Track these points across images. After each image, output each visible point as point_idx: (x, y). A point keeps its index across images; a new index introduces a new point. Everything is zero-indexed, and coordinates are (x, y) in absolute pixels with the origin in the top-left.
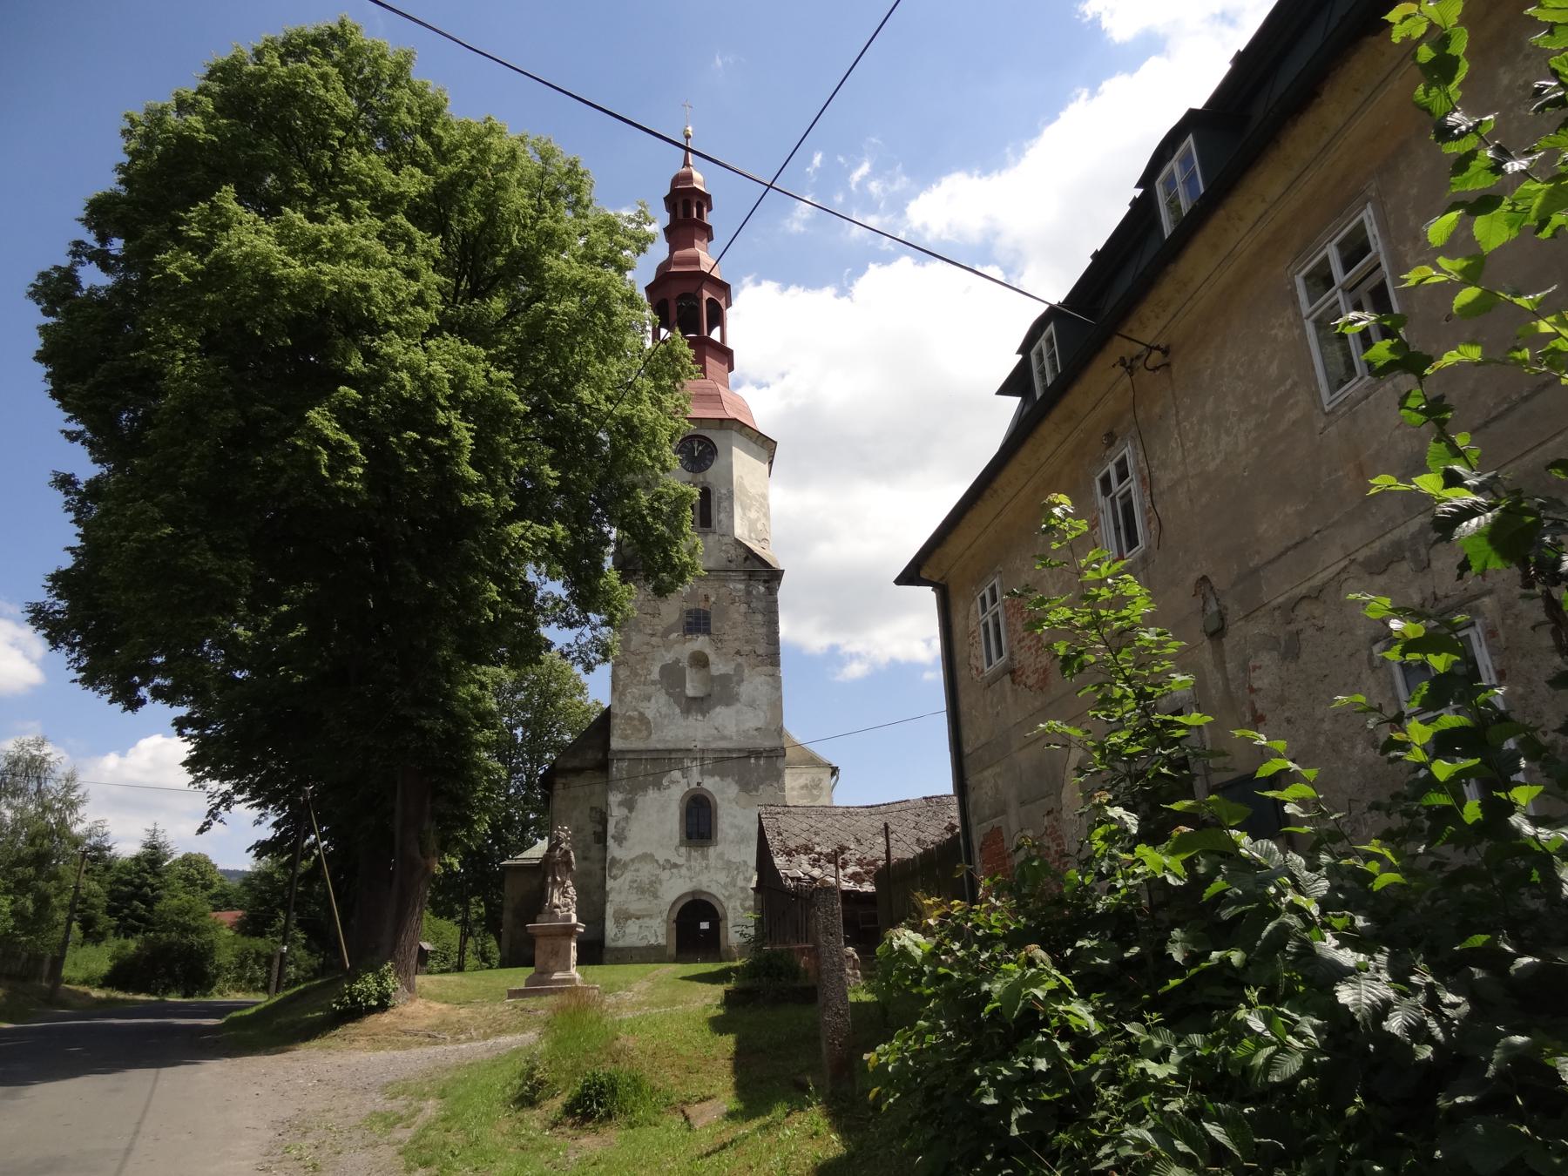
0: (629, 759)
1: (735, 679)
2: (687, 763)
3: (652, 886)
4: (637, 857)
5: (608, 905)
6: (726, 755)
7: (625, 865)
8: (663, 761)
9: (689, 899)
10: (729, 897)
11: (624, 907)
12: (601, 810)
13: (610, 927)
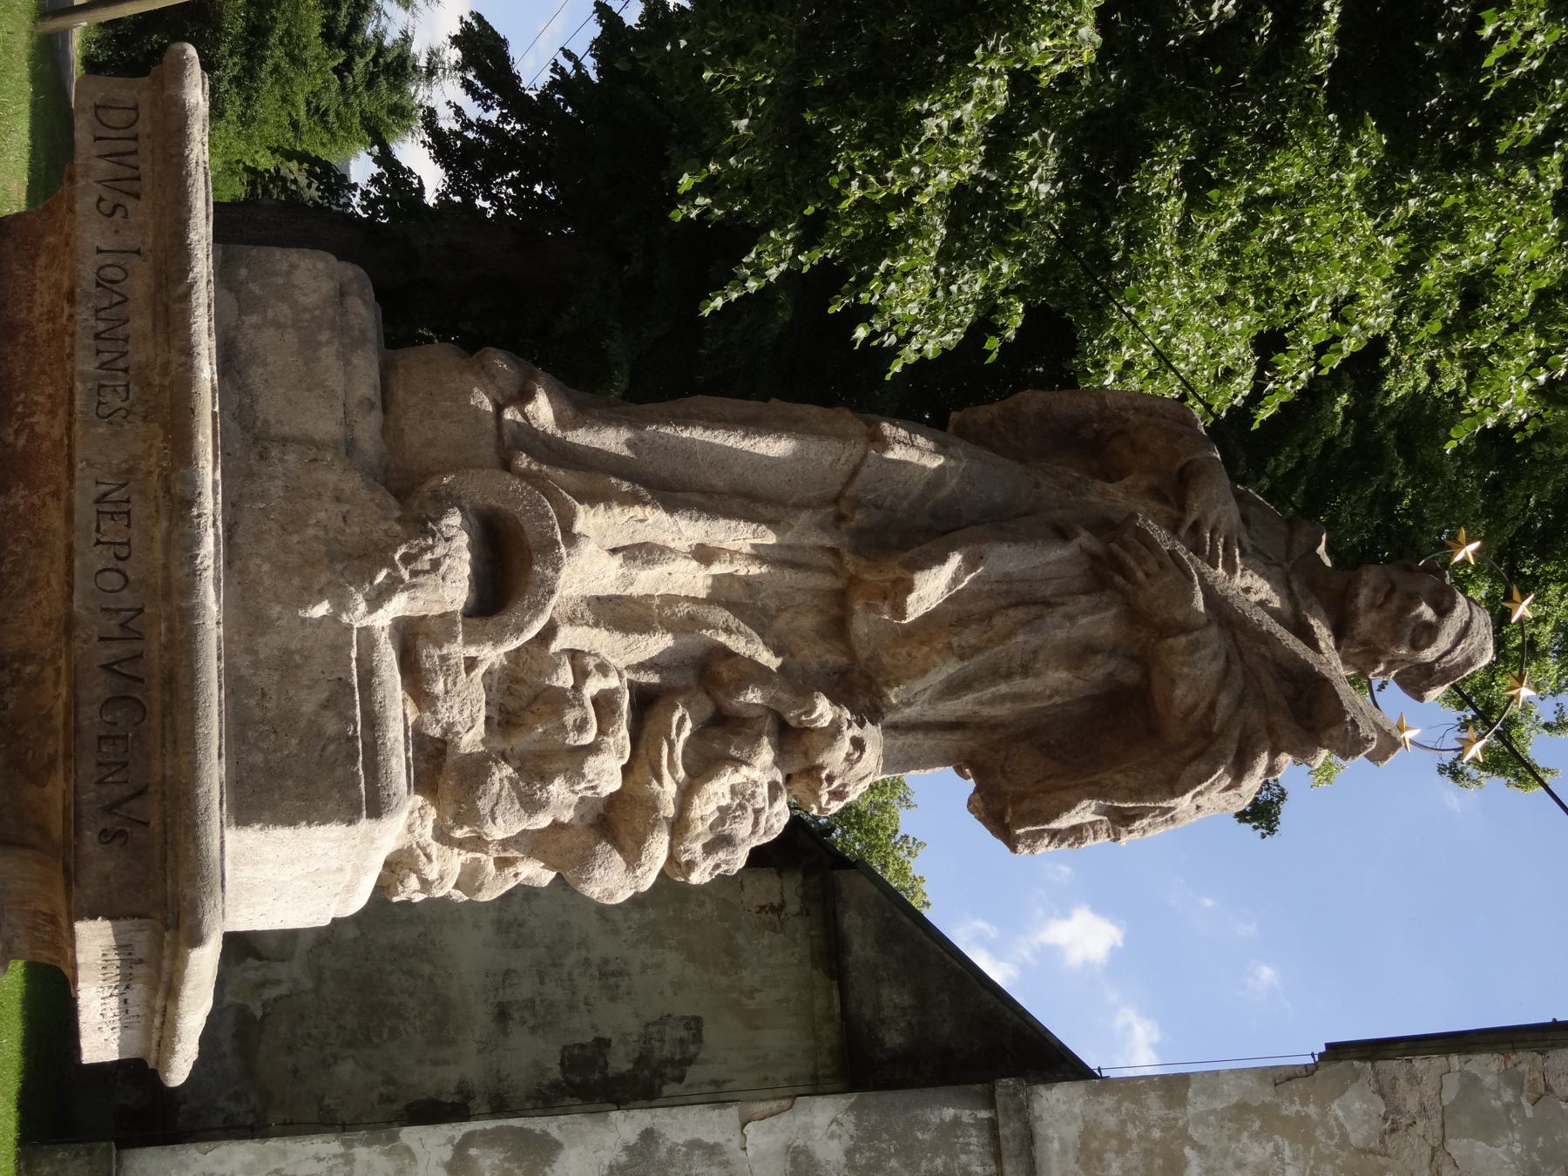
12: (690, 1061)
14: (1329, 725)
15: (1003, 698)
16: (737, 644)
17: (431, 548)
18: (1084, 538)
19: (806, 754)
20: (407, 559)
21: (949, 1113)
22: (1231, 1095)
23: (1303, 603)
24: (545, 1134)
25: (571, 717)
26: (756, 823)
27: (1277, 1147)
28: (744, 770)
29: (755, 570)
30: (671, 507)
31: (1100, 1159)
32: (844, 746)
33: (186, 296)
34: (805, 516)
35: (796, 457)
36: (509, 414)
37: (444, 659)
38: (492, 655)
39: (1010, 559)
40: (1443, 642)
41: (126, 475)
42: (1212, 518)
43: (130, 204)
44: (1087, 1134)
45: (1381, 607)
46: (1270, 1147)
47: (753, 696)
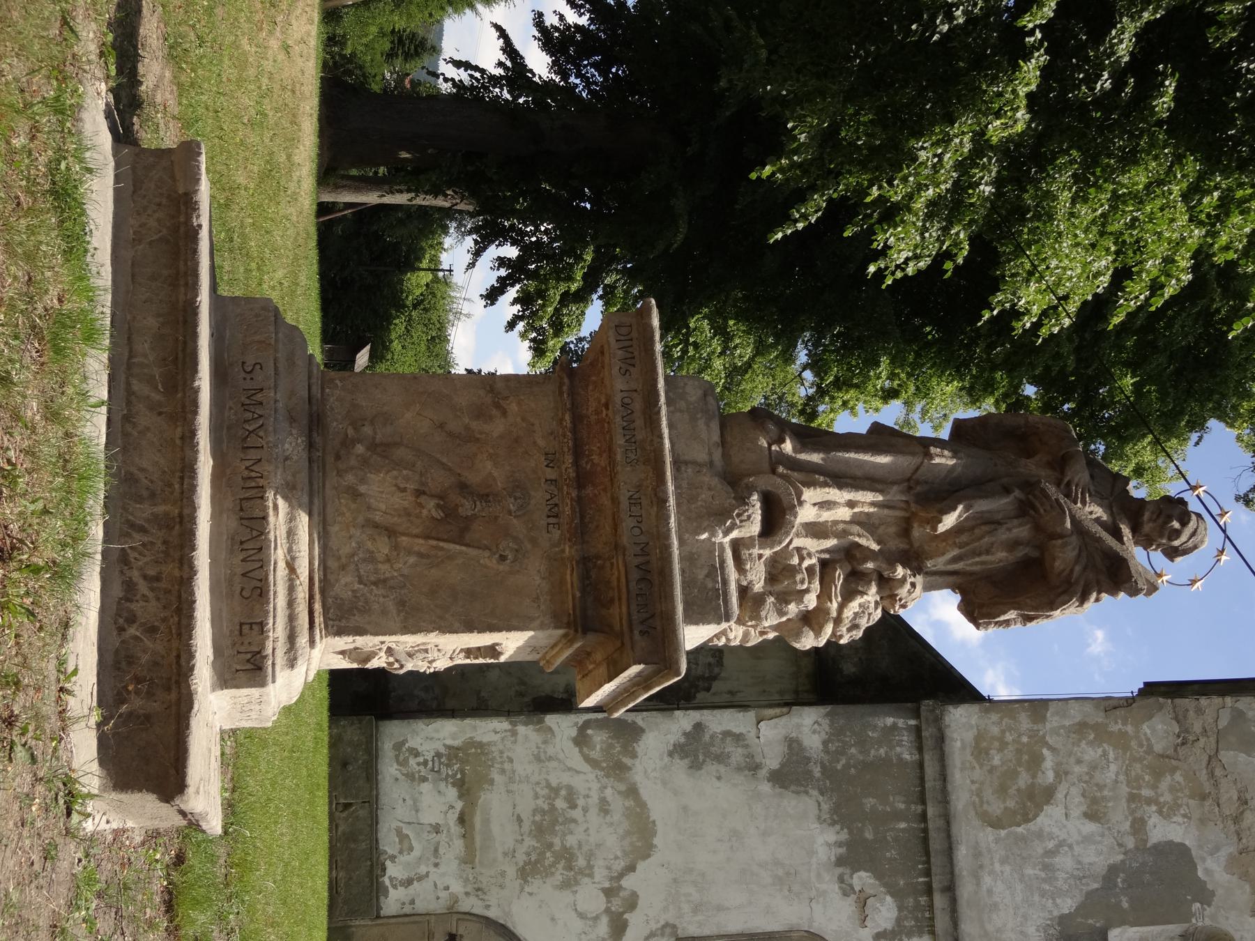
0: (921, 765)
3: (558, 857)
4: (642, 805)
7: (618, 769)
11: (495, 775)
12: (714, 678)
14: (1125, 582)
15: (977, 563)
16: (863, 541)
17: (747, 510)
18: (1017, 493)
19: (891, 589)
20: (739, 515)
21: (890, 721)
22: (1075, 714)
23: (1118, 518)
24: (634, 723)
25: (799, 577)
26: (869, 619)
27: (1104, 751)
28: (865, 597)
29: (872, 510)
30: (840, 487)
31: (987, 754)
32: (908, 586)
33: (659, 412)
34: (895, 488)
35: (892, 463)
36: (774, 448)
37: (750, 555)
38: (767, 553)
39: (983, 505)
40: (1183, 538)
41: (639, 488)
42: (1076, 480)
43: (632, 369)
44: (979, 738)
45: (1155, 521)
46: (1100, 751)
47: (870, 565)
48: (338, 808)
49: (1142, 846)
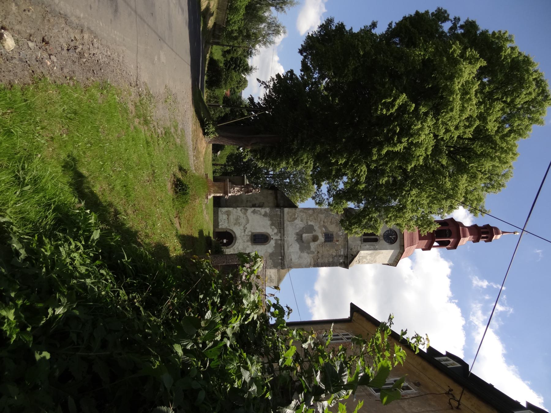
1: (309, 251)
2: (279, 235)
5: (232, 208)
6: (282, 248)
7: (245, 214)
8: (280, 227)
9: (234, 236)
10: (234, 250)
13: (225, 209)
48: (214, 217)
49: (307, 225)
